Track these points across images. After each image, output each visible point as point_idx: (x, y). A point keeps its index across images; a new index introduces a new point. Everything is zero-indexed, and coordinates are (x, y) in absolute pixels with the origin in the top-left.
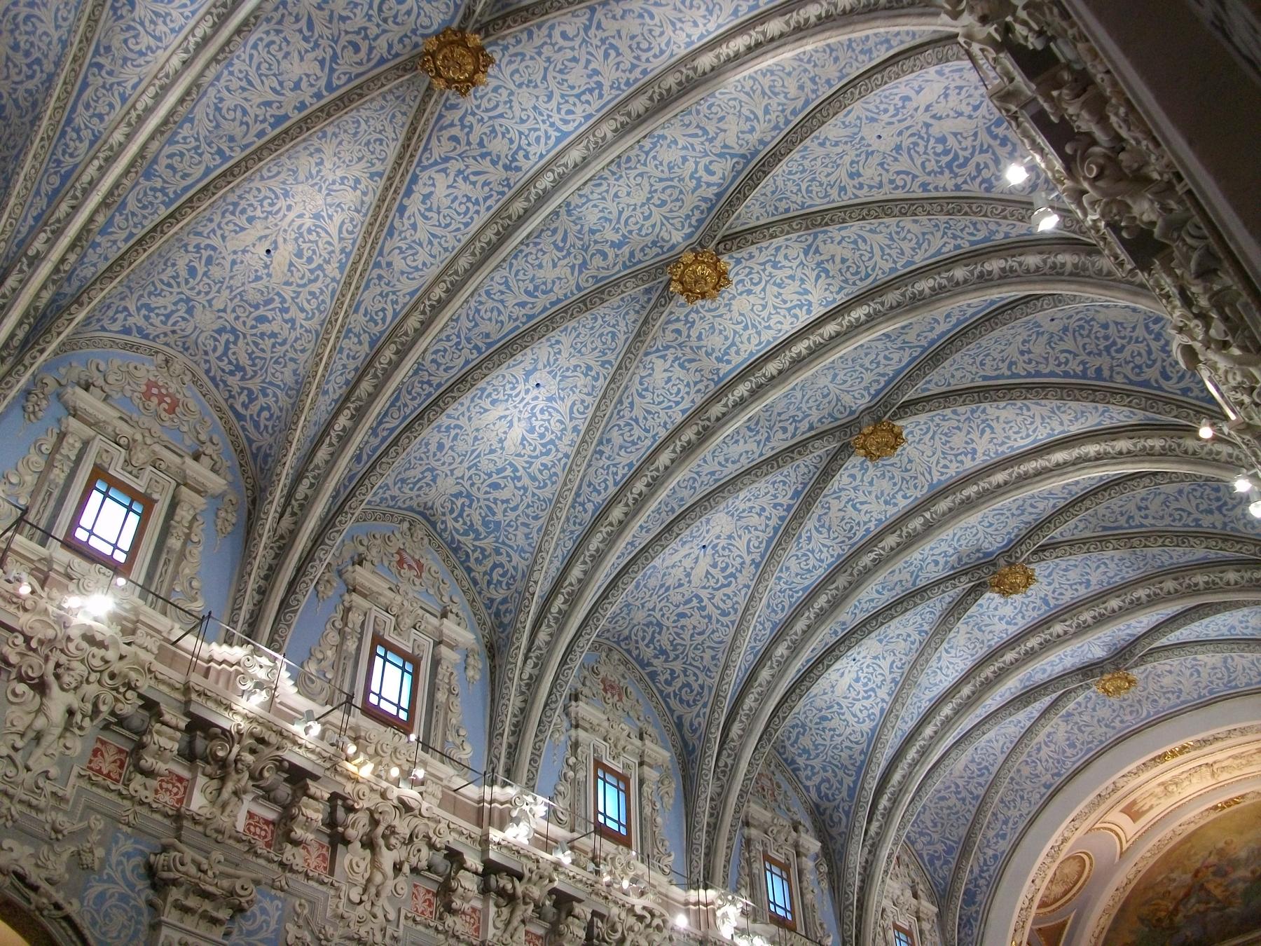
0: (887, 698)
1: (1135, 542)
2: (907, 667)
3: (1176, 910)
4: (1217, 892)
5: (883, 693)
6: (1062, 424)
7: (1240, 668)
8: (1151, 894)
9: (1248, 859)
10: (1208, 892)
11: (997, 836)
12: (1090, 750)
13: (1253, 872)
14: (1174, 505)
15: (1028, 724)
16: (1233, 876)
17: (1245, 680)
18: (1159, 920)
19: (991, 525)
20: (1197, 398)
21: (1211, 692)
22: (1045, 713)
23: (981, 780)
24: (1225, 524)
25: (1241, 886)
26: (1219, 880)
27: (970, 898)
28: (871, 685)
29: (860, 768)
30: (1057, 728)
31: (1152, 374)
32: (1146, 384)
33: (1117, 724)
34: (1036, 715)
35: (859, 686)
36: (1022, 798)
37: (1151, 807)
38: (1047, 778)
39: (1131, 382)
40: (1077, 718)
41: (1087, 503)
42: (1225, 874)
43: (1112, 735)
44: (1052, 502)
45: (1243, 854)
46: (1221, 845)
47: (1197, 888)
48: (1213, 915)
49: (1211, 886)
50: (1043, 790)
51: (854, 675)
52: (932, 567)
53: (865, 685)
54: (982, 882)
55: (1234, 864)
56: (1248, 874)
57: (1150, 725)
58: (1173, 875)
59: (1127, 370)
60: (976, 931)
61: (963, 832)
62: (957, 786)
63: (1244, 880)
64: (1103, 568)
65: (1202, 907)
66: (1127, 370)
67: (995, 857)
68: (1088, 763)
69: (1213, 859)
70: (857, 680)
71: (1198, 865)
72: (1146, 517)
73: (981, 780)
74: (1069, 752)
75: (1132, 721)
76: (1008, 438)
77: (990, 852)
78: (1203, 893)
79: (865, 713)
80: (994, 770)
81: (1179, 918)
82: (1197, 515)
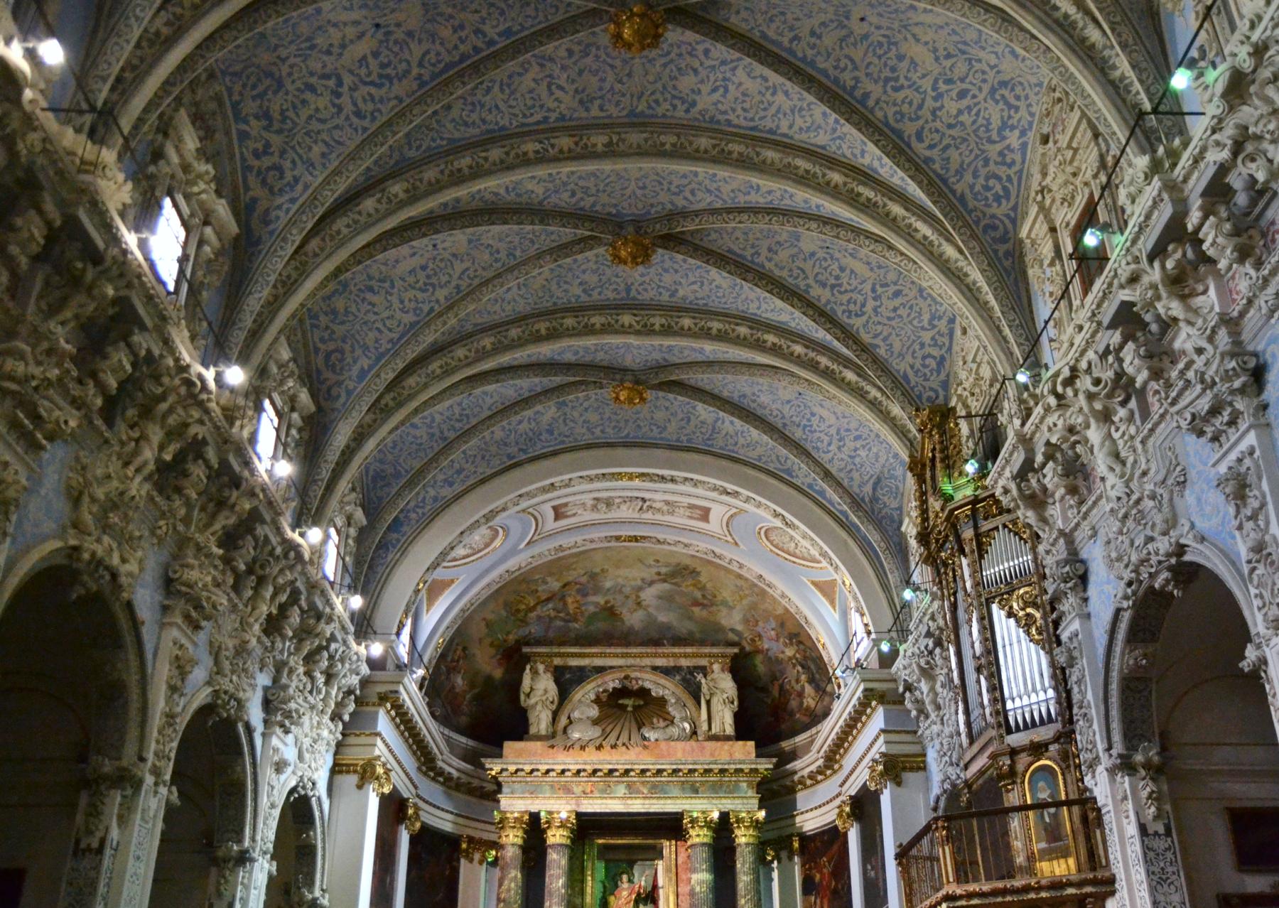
0: (442, 300)
1: (750, 276)
2: (476, 282)
4: (571, 608)
5: (441, 294)
6: (791, 127)
7: (724, 432)
10: (565, 604)
11: (445, 480)
12: (563, 442)
13: (607, 602)
14: (799, 263)
15: (527, 395)
16: (592, 599)
17: (721, 443)
18: (518, 611)
19: (644, 188)
20: (934, 171)
21: (689, 441)
22: (547, 393)
23: (458, 425)
24: (828, 302)
25: (592, 609)
26: (579, 598)
27: (396, 525)
28: (434, 280)
29: (382, 355)
30: (548, 412)
31: (909, 128)
32: (899, 134)
33: (598, 431)
34: (539, 389)
35: (422, 276)
36: (483, 458)
37: (574, 515)
38: (513, 450)
39: (887, 124)
40: (567, 410)
41: (745, 217)
42: (585, 595)
43: (588, 438)
44: (713, 198)
45: (608, 584)
46: (597, 570)
47: (558, 597)
48: (559, 623)
49: (570, 600)
50: (505, 459)
51: (423, 262)
52: (565, 196)
53: (428, 277)
54: (413, 516)
55: (597, 590)
56: (602, 602)
57: (626, 445)
58: (549, 579)
59: (891, 112)
60: (390, 557)
61: (417, 465)
62: (433, 420)
63: (597, 604)
64: (695, 287)
65: (553, 614)
66: (891, 112)
67: (435, 499)
68: (555, 454)
69: (584, 579)
70: (424, 268)
71: (570, 579)
72: (770, 260)
73: (458, 425)
74: (545, 436)
75: (611, 435)
76: (734, 110)
77: (432, 492)
79: (413, 305)
80: (474, 421)
81: (533, 615)
82: (811, 281)
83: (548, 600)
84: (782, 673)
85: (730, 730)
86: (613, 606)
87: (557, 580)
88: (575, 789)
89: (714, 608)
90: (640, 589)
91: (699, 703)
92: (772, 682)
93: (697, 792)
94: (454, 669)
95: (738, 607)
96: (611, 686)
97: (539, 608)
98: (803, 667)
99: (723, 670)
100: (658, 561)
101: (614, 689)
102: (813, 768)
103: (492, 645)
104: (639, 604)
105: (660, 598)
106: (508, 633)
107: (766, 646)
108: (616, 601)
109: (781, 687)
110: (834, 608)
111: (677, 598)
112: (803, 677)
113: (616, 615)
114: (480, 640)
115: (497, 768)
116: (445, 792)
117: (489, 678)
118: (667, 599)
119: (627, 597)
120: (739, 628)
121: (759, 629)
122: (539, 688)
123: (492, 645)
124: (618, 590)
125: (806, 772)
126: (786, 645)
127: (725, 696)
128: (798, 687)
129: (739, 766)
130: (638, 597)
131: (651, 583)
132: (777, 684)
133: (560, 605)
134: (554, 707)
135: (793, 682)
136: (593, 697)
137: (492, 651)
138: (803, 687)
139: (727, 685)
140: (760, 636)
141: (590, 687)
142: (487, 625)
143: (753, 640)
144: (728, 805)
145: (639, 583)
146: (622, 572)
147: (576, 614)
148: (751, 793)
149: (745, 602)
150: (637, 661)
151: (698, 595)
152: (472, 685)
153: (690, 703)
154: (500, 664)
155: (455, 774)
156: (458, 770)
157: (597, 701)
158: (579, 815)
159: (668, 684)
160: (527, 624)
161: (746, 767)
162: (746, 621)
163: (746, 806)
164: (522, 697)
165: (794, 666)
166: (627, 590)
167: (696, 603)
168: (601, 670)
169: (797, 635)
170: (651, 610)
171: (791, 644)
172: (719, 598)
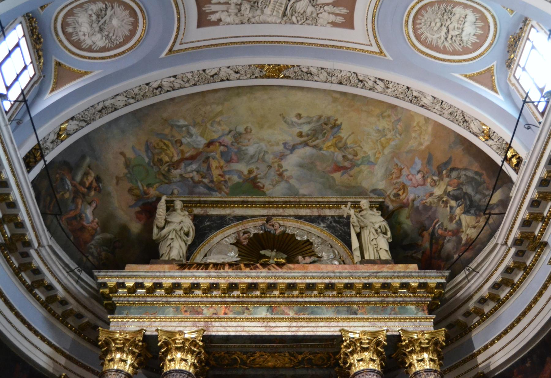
3: (175, 165)
4: (216, 173)
8: (167, 131)
9: (252, 157)
10: (209, 168)
13: (250, 172)
18: (160, 160)
25: (236, 179)
26: (223, 163)
45: (251, 150)
46: (241, 129)
49: (214, 164)
55: (241, 155)
56: (246, 172)
58: (193, 130)
63: (240, 173)
65: (197, 178)
69: (228, 140)
71: (215, 136)
78: (205, 166)
81: (176, 172)
83: (193, 158)
84: (432, 219)
85: (385, 256)
86: (256, 177)
87: (202, 135)
88: (205, 311)
89: (356, 169)
90: (282, 156)
91: (349, 245)
92: (421, 235)
93: (356, 314)
94: (84, 195)
95: (380, 161)
96: (253, 231)
97: (183, 165)
98: (456, 198)
99: (371, 208)
100: (299, 116)
101: (255, 234)
102: (497, 277)
103: (130, 190)
104: (281, 175)
105: (301, 166)
106: (149, 186)
107: (411, 197)
108: (260, 170)
109: (432, 235)
110: (496, 92)
111: (318, 163)
112: (458, 211)
113: (259, 187)
114: (118, 179)
115: (112, 283)
116: (45, 319)
117: (124, 229)
118: (307, 166)
119: (270, 167)
120: (381, 185)
121: (403, 179)
122: (175, 227)
123: (130, 190)
124: (259, 157)
125: (485, 291)
126: (435, 184)
127: (377, 226)
128: (452, 226)
129: (404, 281)
130: (280, 166)
131: (293, 148)
132: (426, 234)
133: (204, 167)
134: (190, 240)
135: (447, 224)
136: (233, 241)
137: (131, 199)
138: (459, 223)
139: (377, 219)
140: (404, 187)
141: (229, 232)
142: (127, 165)
143: (397, 195)
144: (394, 327)
145: (281, 147)
146: (266, 133)
147: (220, 182)
148: (420, 315)
149: (386, 151)
150: (280, 211)
151: (339, 156)
152: (104, 227)
153: (338, 245)
154: (139, 219)
155: (61, 293)
156: (65, 288)
157: (237, 244)
158: (208, 340)
159: (313, 230)
160: (170, 182)
161: (414, 283)
162: (388, 175)
163: (419, 326)
164: (155, 230)
165: (446, 203)
166: (269, 158)
167: (338, 168)
168: (242, 218)
169: (446, 163)
170: (292, 181)
171: (441, 179)
172: (361, 155)
